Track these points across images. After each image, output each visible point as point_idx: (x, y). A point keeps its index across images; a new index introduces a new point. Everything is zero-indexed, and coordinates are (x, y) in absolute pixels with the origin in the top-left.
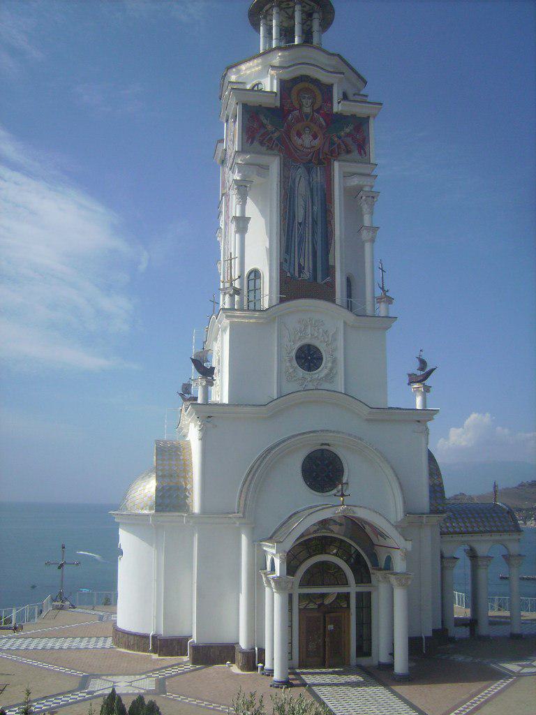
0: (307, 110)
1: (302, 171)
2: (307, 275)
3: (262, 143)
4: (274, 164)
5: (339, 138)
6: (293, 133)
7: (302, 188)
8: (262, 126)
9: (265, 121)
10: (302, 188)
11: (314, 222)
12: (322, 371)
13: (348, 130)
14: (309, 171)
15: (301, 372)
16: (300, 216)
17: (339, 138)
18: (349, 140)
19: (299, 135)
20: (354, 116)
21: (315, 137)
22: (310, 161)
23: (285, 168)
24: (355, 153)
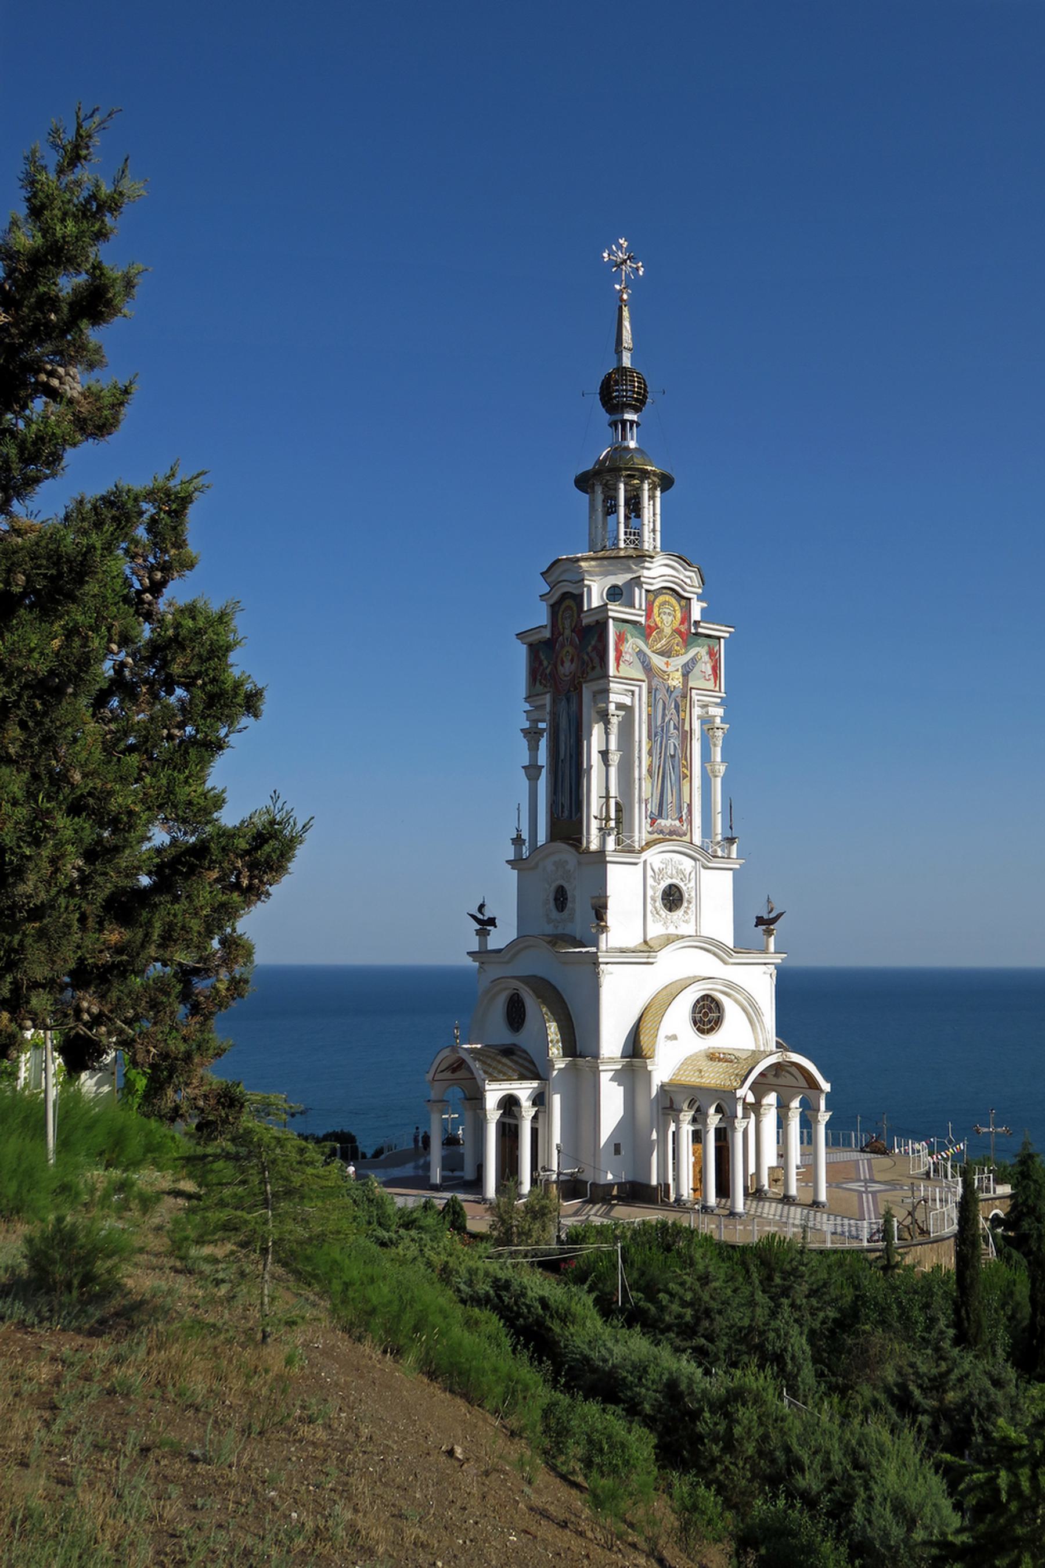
0: (567, 632)
1: (564, 703)
2: (566, 813)
3: (541, 683)
4: (547, 699)
5: (588, 654)
6: (559, 663)
7: (564, 723)
8: (541, 663)
9: (543, 657)
10: (564, 723)
11: (571, 756)
12: (566, 912)
13: (593, 643)
14: (568, 700)
15: (555, 914)
16: (562, 756)
17: (588, 654)
18: (594, 655)
19: (562, 665)
20: (597, 622)
21: (572, 661)
22: (569, 691)
23: (554, 702)
24: (598, 668)
